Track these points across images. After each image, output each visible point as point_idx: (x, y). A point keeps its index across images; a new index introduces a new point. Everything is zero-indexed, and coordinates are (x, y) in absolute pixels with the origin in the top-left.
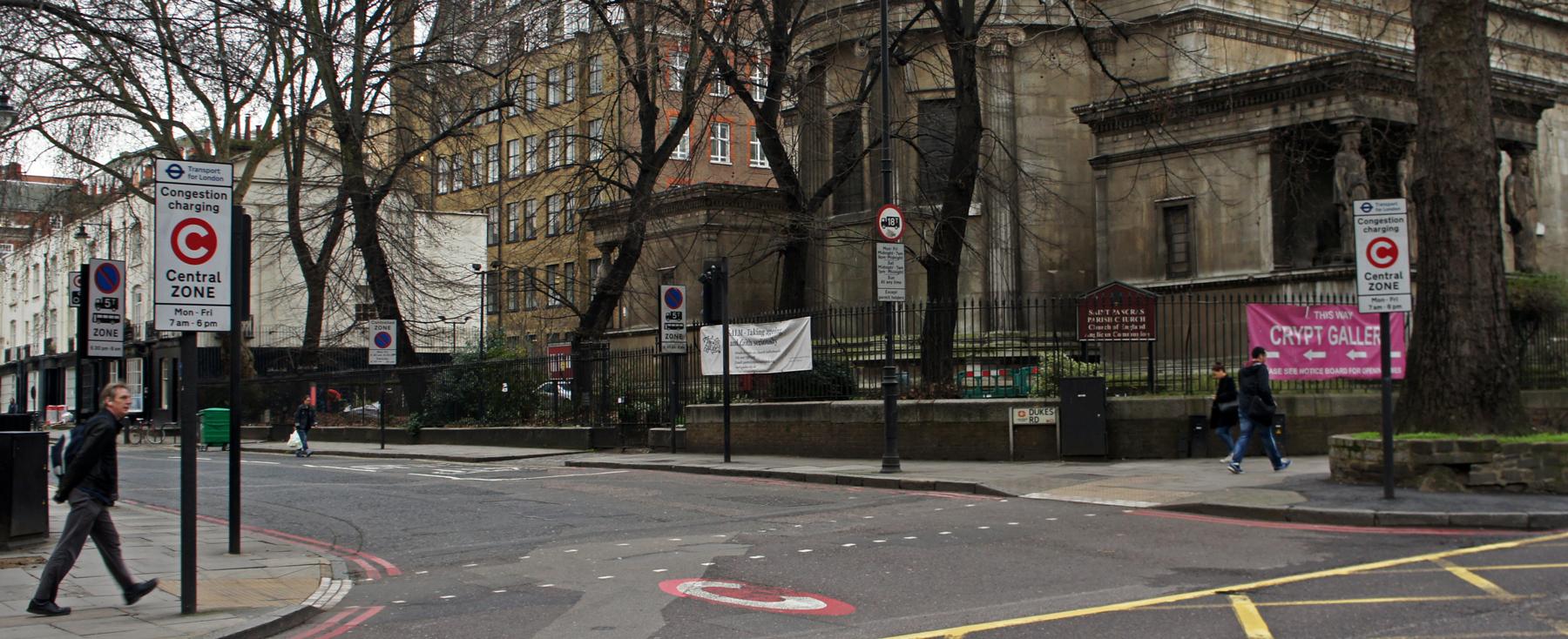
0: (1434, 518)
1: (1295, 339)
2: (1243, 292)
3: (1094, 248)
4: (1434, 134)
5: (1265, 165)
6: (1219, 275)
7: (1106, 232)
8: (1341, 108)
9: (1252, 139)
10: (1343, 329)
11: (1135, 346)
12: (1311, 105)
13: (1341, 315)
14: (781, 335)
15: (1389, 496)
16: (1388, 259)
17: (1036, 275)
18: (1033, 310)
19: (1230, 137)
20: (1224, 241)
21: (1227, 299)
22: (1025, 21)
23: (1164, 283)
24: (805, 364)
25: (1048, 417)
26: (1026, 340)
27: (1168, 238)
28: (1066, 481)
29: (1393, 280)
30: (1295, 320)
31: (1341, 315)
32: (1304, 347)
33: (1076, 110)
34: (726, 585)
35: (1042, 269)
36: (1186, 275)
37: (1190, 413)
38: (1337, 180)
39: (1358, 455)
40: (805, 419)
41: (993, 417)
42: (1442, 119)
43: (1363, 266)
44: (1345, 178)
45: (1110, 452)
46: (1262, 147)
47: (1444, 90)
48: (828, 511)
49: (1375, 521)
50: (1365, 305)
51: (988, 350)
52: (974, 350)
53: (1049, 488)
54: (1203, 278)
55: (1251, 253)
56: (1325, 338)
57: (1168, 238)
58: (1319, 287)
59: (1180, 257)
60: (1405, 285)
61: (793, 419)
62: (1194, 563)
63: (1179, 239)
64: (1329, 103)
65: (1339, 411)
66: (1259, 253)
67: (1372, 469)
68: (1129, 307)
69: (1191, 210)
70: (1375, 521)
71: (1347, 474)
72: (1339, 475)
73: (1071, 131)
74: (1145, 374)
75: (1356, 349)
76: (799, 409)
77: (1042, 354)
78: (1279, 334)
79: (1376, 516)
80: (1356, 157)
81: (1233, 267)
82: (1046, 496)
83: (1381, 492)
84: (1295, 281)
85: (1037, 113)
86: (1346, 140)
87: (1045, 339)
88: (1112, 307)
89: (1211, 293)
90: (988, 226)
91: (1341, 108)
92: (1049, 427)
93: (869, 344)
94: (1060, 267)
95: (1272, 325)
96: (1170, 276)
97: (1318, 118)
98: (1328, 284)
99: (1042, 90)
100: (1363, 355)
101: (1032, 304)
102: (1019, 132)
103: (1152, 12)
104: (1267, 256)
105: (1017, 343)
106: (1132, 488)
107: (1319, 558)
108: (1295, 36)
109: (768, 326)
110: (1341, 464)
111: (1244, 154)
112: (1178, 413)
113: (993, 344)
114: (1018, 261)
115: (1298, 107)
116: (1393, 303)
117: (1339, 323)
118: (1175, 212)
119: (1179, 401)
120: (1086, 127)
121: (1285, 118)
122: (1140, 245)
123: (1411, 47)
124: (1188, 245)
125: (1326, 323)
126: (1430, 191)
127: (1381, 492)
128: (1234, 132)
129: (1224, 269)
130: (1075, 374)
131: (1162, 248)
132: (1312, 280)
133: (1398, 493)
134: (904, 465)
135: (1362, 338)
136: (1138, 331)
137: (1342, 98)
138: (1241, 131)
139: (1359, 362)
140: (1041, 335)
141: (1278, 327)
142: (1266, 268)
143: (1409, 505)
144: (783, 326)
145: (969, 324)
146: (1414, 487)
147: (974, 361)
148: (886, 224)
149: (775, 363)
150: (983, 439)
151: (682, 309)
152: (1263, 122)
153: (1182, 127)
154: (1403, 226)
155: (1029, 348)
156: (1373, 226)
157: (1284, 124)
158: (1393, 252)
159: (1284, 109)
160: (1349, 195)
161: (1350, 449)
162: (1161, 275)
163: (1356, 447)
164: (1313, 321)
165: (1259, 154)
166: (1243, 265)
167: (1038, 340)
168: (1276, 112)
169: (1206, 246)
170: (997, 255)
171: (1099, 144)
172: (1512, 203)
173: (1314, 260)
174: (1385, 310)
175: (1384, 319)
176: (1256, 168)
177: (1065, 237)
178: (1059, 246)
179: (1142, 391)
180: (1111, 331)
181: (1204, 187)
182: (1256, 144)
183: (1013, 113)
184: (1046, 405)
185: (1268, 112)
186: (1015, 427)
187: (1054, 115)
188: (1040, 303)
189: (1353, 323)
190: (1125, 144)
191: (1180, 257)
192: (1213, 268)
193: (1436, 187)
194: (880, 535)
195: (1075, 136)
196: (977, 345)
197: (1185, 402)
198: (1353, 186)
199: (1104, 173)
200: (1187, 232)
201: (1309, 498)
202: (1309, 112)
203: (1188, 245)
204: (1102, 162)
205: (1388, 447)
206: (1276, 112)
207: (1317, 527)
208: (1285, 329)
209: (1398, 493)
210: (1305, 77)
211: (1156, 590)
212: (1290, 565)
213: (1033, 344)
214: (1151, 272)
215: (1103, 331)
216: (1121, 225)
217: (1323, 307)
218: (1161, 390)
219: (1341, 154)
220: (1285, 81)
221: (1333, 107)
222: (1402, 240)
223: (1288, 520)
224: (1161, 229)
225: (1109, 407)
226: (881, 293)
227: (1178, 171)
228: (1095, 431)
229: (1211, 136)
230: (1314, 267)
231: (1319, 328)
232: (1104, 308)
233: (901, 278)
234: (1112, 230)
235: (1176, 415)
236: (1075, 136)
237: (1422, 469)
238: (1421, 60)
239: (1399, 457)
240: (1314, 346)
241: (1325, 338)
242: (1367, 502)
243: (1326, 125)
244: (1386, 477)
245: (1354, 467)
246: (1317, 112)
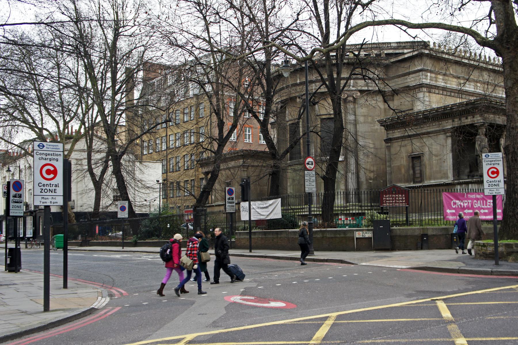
0: (514, 272)
1: (461, 205)
2: (441, 188)
3: (386, 172)
4: (513, 128)
5: (449, 141)
6: (433, 182)
7: (390, 166)
8: (478, 119)
9: (445, 131)
10: (479, 201)
11: (401, 208)
12: (467, 118)
13: (478, 196)
14: (270, 205)
15: (497, 264)
16: (495, 175)
17: (365, 182)
18: (363, 195)
19: (436, 131)
20: (434, 169)
21: (435, 191)
22: (359, 88)
23: (412, 185)
24: (279, 216)
25: (369, 235)
26: (361, 206)
27: (414, 168)
28: (375, 258)
29: (497, 183)
30: (461, 198)
31: (478, 196)
32: (464, 209)
33: (379, 121)
34: (249, 298)
35: (367, 180)
36: (420, 182)
38: (477, 146)
39: (485, 248)
40: (279, 236)
41: (349, 235)
42: (515, 123)
43: (486, 178)
44: (480, 145)
45: (393, 249)
46: (448, 134)
47: (516, 111)
48: (287, 270)
49: (492, 273)
50: (487, 192)
51: (347, 210)
52: (341, 210)
53: (369, 261)
54: (426, 183)
55: (444, 174)
56: (472, 205)
57: (414, 168)
58: (470, 185)
59: (418, 175)
60: (502, 185)
61: (275, 236)
62: (423, 289)
63: (417, 169)
64: (474, 117)
66: (447, 174)
67: (490, 254)
68: (399, 194)
69: (422, 158)
70: (492, 273)
71: (481, 256)
72: (478, 256)
73: (377, 129)
74: (405, 219)
75: (484, 209)
76: (277, 233)
77: (366, 211)
78: (455, 204)
79: (492, 271)
80: (483, 137)
81: (437, 179)
82: (368, 264)
83: (494, 262)
84: (460, 184)
85: (364, 123)
86: (480, 131)
87: (368, 206)
88: (392, 194)
89: (429, 189)
90: (347, 164)
91: (478, 119)
93: (303, 209)
94: (373, 180)
95: (452, 200)
96: (414, 183)
98: (473, 185)
99: (366, 114)
100: (486, 211)
101: (363, 193)
102: (358, 129)
103: (407, 85)
104: (450, 174)
105: (357, 208)
106: (400, 261)
107: (470, 287)
108: (460, 92)
109: (265, 202)
110: (478, 252)
111: (442, 137)
112: (417, 233)
113: (348, 208)
114: (358, 177)
116: (497, 192)
117: (477, 199)
118: (416, 159)
119: (418, 229)
120: (383, 127)
121: (457, 123)
122: (403, 171)
123: (504, 96)
124: (421, 171)
125: (472, 199)
126: (511, 149)
127: (494, 262)
128: (438, 129)
129: (434, 180)
130: (379, 219)
131: (411, 172)
132: (467, 183)
133: (500, 263)
134: (316, 253)
135: (486, 205)
136: (402, 203)
137: (478, 116)
138: (440, 128)
139: (485, 214)
140: (366, 205)
141: (454, 201)
142: (450, 179)
143: (505, 267)
144: (271, 202)
145: (339, 201)
146: (507, 261)
147: (341, 214)
148: (308, 164)
149: (268, 215)
150: (345, 243)
151: (234, 196)
152: (448, 125)
153: (418, 127)
154: (501, 163)
155: (362, 209)
156: (489, 163)
157: (456, 125)
158: (497, 172)
159: (456, 120)
160: (481, 152)
161: (482, 246)
162: (411, 182)
163: (484, 245)
164: (468, 199)
165: (447, 137)
166: (442, 178)
167: (365, 206)
168: (453, 121)
169: (427, 172)
170: (350, 175)
171: (387, 134)
173: (468, 176)
174: (494, 194)
175: (494, 197)
176: (446, 143)
177: (375, 168)
178: (373, 172)
179: (403, 225)
180: (392, 203)
181: (427, 149)
182: (445, 133)
183: (355, 123)
184: (368, 230)
185: (450, 121)
186: (357, 238)
187: (371, 123)
188: (366, 193)
189: (483, 199)
190: (397, 134)
191: (418, 175)
192: (430, 179)
193: (514, 148)
194: (306, 279)
195: (379, 131)
196: (342, 208)
197: (420, 229)
198: (483, 148)
199: (389, 144)
200: (420, 166)
201: (467, 264)
202: (466, 121)
203: (421, 171)
204: (388, 141)
205: (496, 245)
206: (453, 121)
207: (469, 275)
208: (457, 201)
209: (500, 263)
210: (464, 108)
211: (409, 299)
212: (459, 290)
213: (363, 208)
214: (407, 181)
215: (389, 203)
216: (396, 163)
217: (471, 194)
218: (411, 224)
219: (478, 137)
220: (457, 109)
221: (475, 119)
222: (500, 168)
223: (458, 273)
224: (411, 165)
225: (391, 231)
226: (307, 189)
227: (417, 143)
228: (386, 240)
229: (429, 130)
230: (468, 179)
231: (470, 201)
232: (389, 194)
233: (314, 184)
234: (392, 165)
235: (416, 234)
236: (379, 131)
237: (510, 254)
238: (508, 101)
239: (500, 249)
240: (468, 208)
241: (472, 205)
242: (488, 266)
243: (472, 126)
244: (495, 256)
245: (483, 253)
246: (468, 121)
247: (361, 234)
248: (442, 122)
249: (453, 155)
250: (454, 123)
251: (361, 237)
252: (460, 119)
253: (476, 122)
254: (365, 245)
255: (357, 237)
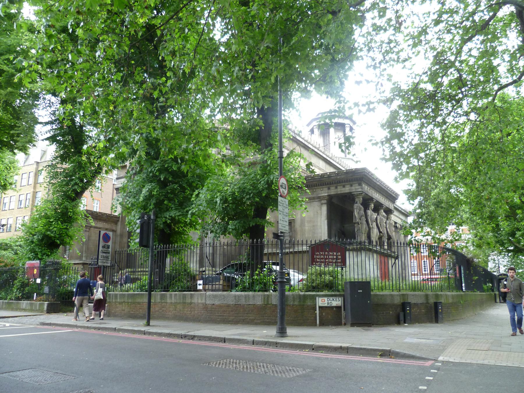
5: (324, 208)
9: (320, 198)
37: (402, 302)
41: (309, 303)
44: (359, 213)
46: (323, 202)
64: (351, 186)
65: (451, 301)
86: (356, 200)
91: (355, 188)
92: (338, 308)
97: (347, 191)
111: (316, 204)
115: (339, 187)
121: (333, 191)
151: (110, 243)
152: (324, 193)
157: (332, 193)
165: (322, 204)
168: (329, 189)
172: (389, 230)
176: (321, 209)
182: (321, 200)
186: (320, 307)
198: (362, 216)
202: (343, 189)
206: (329, 189)
220: (335, 178)
221: (353, 188)
246: (347, 189)
247: (326, 302)
248: (317, 190)
249: (328, 222)
250: (329, 191)
251: (326, 305)
252: (336, 188)
253: (354, 190)
254: (332, 318)
255: (321, 305)
